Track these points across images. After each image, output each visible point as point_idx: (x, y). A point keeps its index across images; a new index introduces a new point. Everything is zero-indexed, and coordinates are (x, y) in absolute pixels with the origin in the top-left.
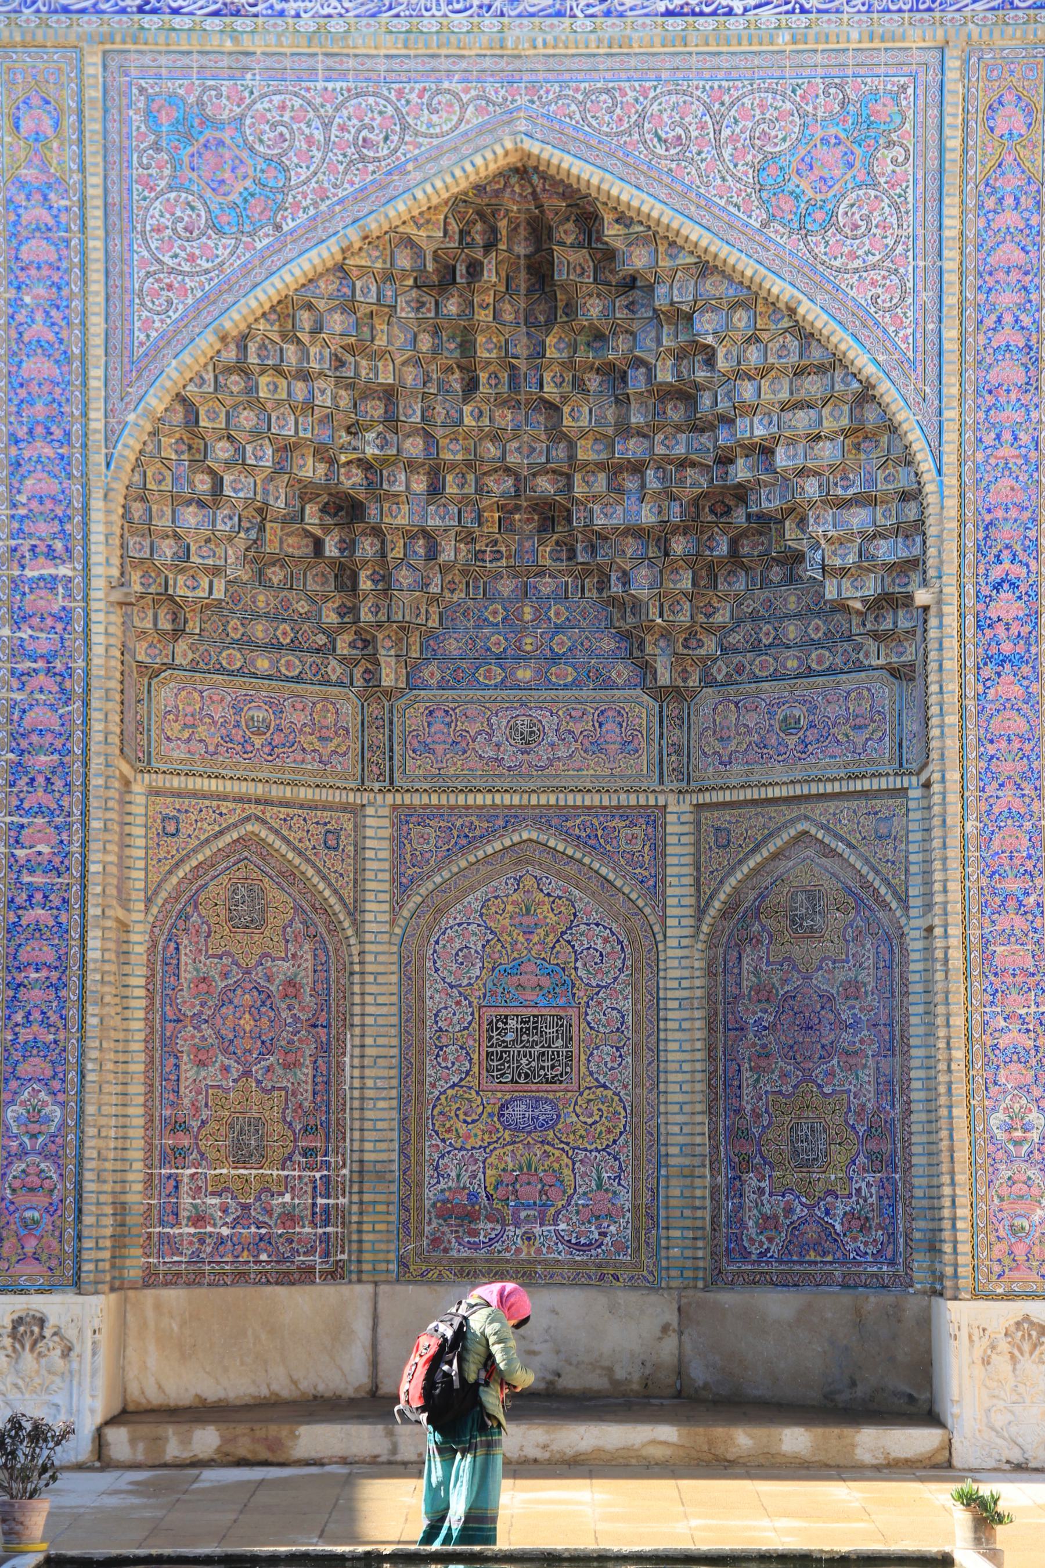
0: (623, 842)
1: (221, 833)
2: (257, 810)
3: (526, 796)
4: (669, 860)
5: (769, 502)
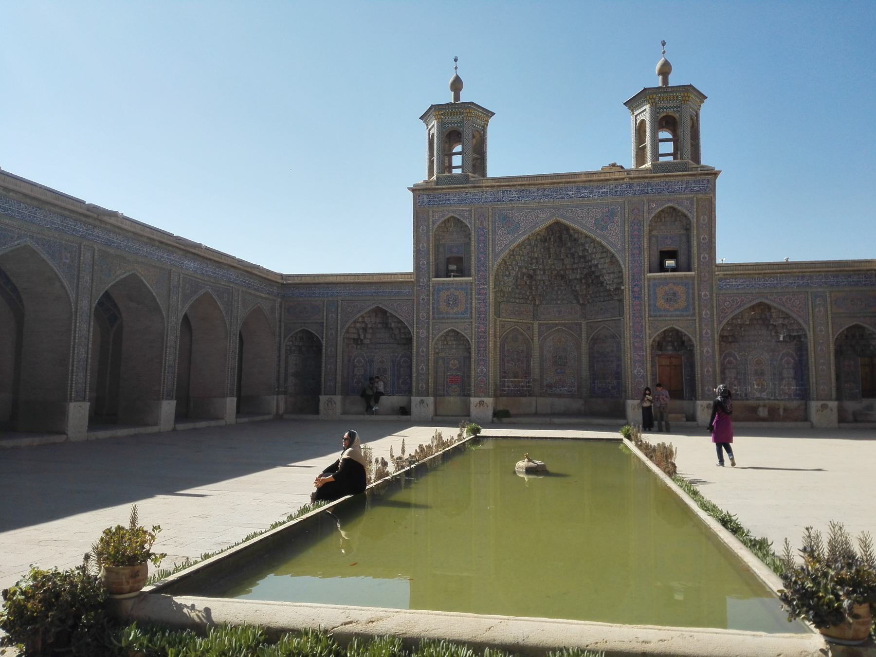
5: (597, 274)
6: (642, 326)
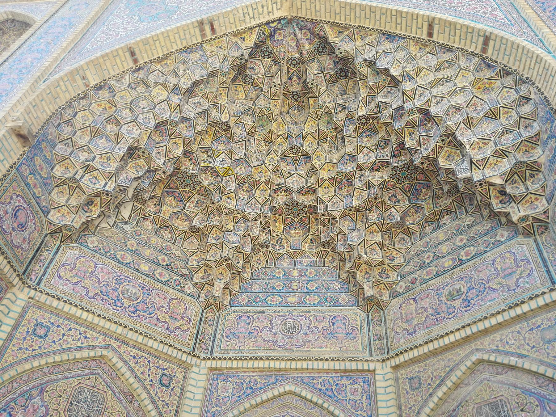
0: (349, 394)
1: (82, 348)
2: (116, 345)
3: (289, 362)
4: (380, 404)
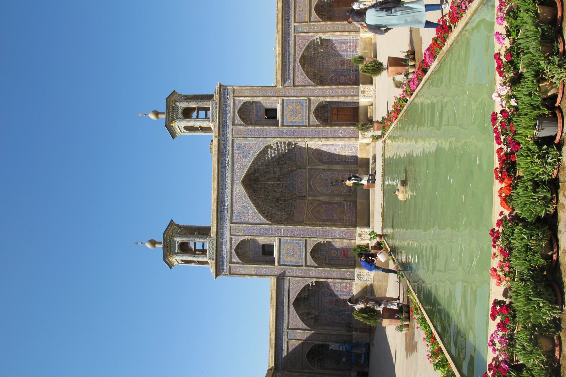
6: (312, 131)
